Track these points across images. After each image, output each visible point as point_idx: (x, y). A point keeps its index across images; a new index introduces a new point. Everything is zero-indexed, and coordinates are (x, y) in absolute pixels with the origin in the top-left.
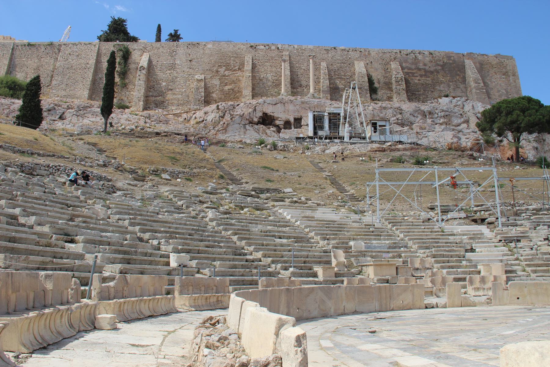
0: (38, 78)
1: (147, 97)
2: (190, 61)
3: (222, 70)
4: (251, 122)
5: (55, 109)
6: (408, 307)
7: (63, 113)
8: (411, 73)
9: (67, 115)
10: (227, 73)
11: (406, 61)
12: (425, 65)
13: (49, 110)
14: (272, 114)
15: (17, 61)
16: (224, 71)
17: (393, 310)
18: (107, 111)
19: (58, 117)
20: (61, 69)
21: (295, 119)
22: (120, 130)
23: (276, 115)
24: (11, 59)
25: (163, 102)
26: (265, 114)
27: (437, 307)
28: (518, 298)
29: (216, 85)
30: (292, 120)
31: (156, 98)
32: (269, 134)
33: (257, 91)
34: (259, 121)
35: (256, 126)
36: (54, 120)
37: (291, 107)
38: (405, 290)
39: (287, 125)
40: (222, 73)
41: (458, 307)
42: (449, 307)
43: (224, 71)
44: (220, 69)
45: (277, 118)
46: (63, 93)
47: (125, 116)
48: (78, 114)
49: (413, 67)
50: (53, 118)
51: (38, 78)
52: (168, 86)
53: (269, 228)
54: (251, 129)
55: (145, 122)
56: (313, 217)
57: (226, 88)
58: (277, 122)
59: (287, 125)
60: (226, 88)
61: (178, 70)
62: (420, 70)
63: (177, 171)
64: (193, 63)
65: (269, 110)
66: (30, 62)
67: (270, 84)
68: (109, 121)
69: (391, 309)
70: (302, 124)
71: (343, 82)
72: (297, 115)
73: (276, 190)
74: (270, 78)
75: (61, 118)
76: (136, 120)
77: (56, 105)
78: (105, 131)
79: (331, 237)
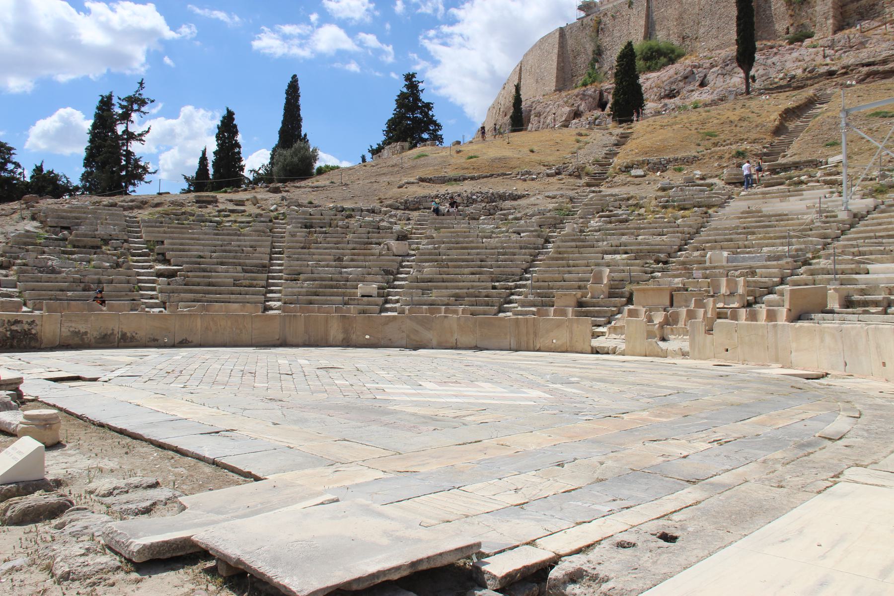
0: (630, 44)
1: (842, 7)
5: (693, 73)
6: (564, 349)
7: (705, 76)
9: (710, 77)
13: (686, 78)
15: (655, 15)
17: (538, 350)
18: (745, 58)
19: (697, 84)
20: (707, 7)
22: (776, 83)
24: (648, 16)
27: (614, 353)
28: (727, 350)
36: (692, 91)
38: (559, 325)
41: (641, 355)
42: (619, 354)
46: (716, 42)
47: (795, 54)
48: (725, 72)
50: (691, 88)
51: (630, 44)
53: (624, 239)
55: (824, 57)
56: (760, 212)
63: (665, 160)
66: (670, 11)
68: (752, 73)
69: (538, 347)
73: (811, 161)
75: (703, 84)
76: (813, 56)
77: (695, 67)
78: (748, 93)
79: (707, 245)
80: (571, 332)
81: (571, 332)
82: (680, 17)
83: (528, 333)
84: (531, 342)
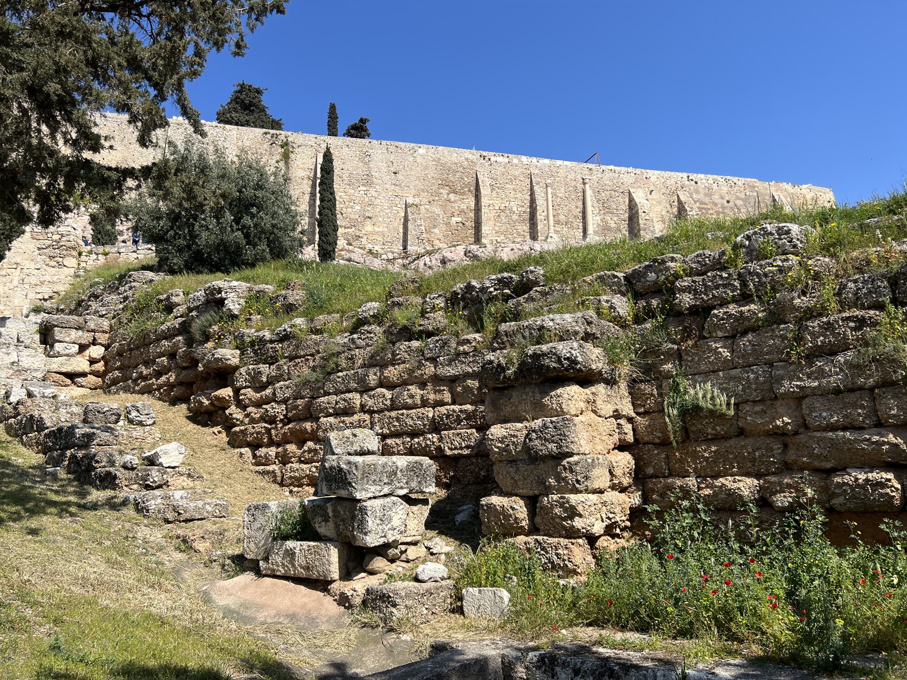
2: (395, 173)
3: (444, 191)
8: (704, 208)
10: (452, 197)
11: (697, 192)
12: (722, 198)
16: (448, 194)
29: (438, 215)
31: (346, 230)
33: (497, 228)
43: (448, 194)
44: (442, 191)
49: (707, 200)
60: (454, 220)
61: (378, 187)
62: (716, 205)
64: (399, 176)
67: (515, 217)
71: (615, 219)
74: (515, 209)
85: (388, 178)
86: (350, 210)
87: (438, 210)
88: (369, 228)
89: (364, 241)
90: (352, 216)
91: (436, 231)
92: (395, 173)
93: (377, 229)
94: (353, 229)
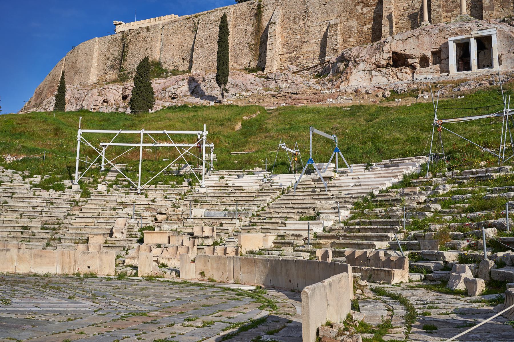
0: (146, 59)
2: (324, 5)
3: (359, 8)
4: (379, 66)
14: (403, 52)
16: (362, 8)
21: (433, 53)
23: (408, 52)
25: (298, 57)
26: (394, 53)
29: (353, 27)
30: (429, 55)
32: (400, 77)
33: (400, 25)
34: (388, 64)
35: (384, 70)
37: (426, 39)
39: (424, 61)
40: (360, 11)
43: (362, 8)
44: (357, 8)
45: (410, 57)
52: (302, 38)
54: (377, 74)
57: (365, 28)
58: (410, 61)
59: (424, 61)
60: (365, 28)
65: (399, 48)
70: (442, 58)
72: (435, 47)
80: (101, 261)
81: (101, 261)
82: (182, 45)
83: (70, 262)
84: (72, 268)
85: (319, 9)
86: (293, 40)
87: (354, 23)
88: (305, 49)
89: (301, 59)
90: (294, 44)
91: (352, 39)
92: (324, 5)
93: (310, 49)
94: (295, 53)
